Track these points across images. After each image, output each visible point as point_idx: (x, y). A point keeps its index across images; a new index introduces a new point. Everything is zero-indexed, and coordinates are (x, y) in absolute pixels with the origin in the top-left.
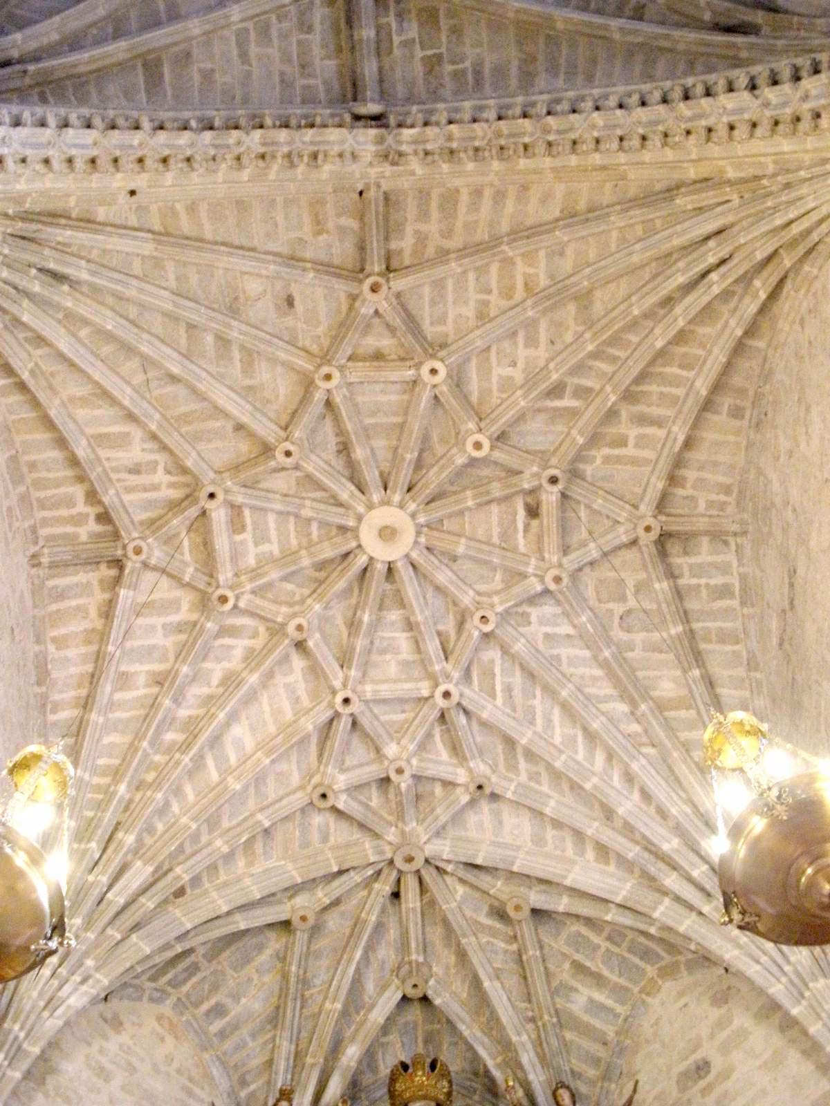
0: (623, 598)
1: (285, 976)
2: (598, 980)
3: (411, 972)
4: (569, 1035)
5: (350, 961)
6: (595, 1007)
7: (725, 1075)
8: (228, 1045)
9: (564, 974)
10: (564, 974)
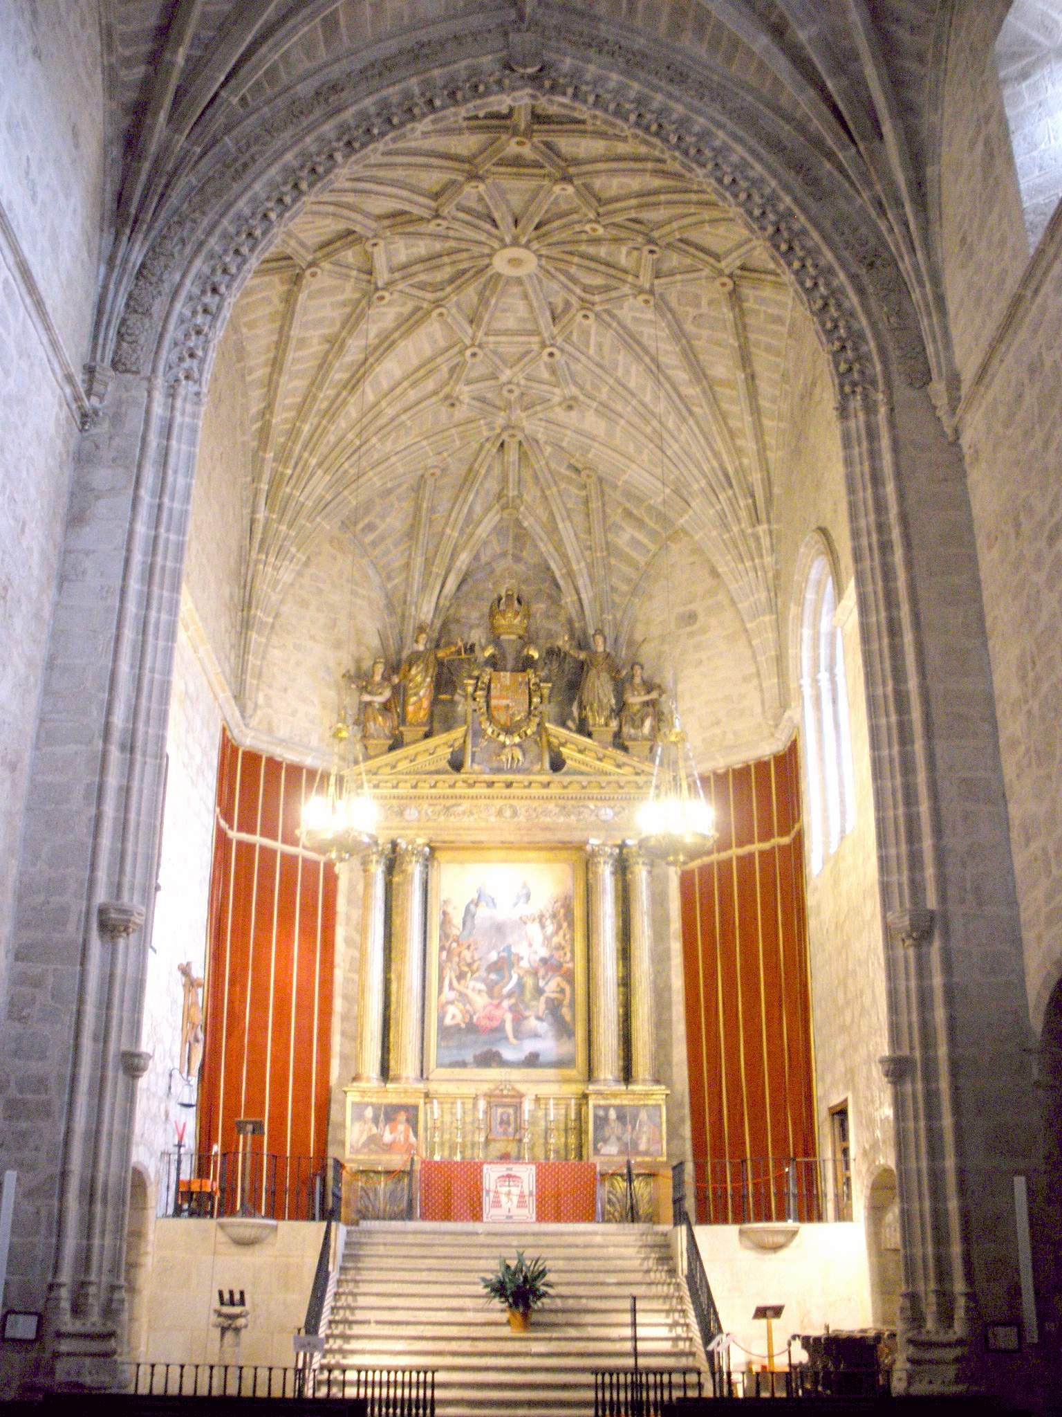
0: (698, 306)
1: (418, 508)
2: (640, 524)
3: (507, 503)
4: (613, 561)
5: (465, 500)
6: (635, 542)
7: (704, 630)
8: (377, 552)
9: (616, 516)
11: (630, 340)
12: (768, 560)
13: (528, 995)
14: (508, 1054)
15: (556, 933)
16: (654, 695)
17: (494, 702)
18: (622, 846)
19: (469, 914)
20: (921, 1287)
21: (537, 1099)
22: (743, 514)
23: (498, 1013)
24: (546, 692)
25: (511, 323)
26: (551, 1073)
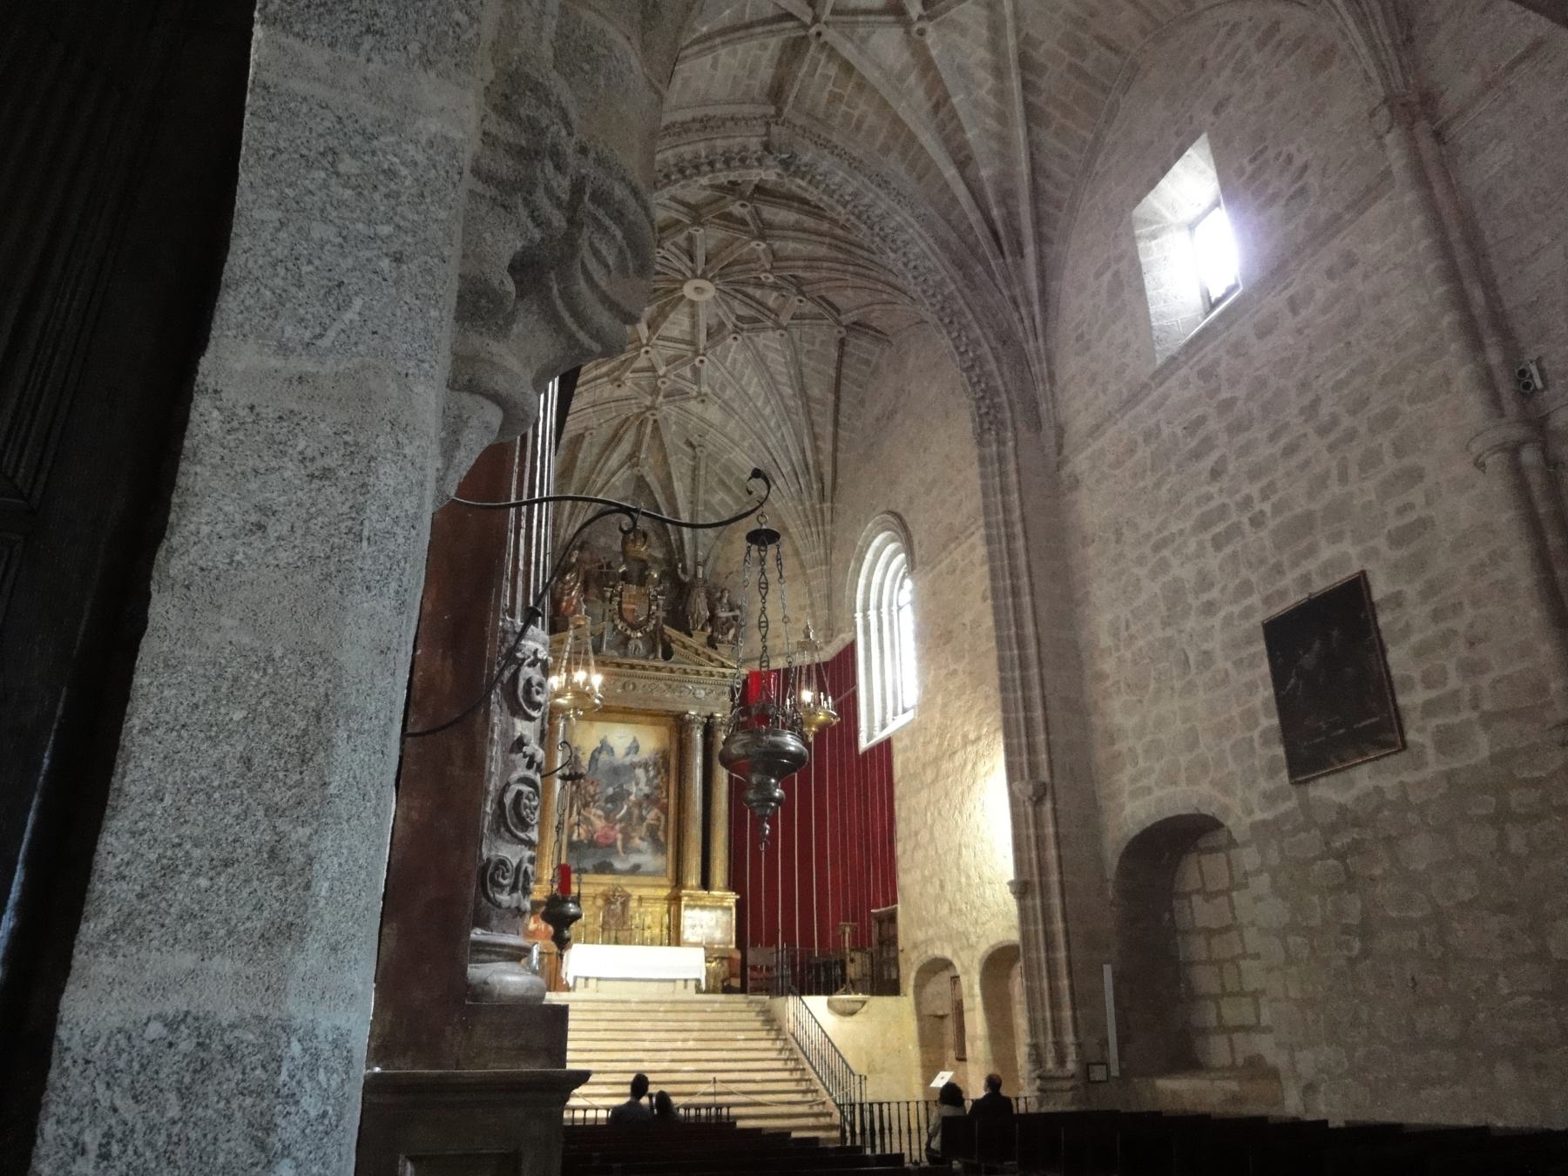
0: (813, 344)
2: (728, 489)
10: (714, 483)
11: (760, 361)
12: (828, 528)
13: (635, 820)
14: (618, 865)
15: (655, 777)
16: (737, 612)
17: (624, 606)
18: (711, 716)
19: (594, 759)
20: (1041, 1040)
21: (641, 899)
22: (815, 494)
23: (612, 833)
24: (661, 602)
25: (675, 333)
26: (649, 880)
